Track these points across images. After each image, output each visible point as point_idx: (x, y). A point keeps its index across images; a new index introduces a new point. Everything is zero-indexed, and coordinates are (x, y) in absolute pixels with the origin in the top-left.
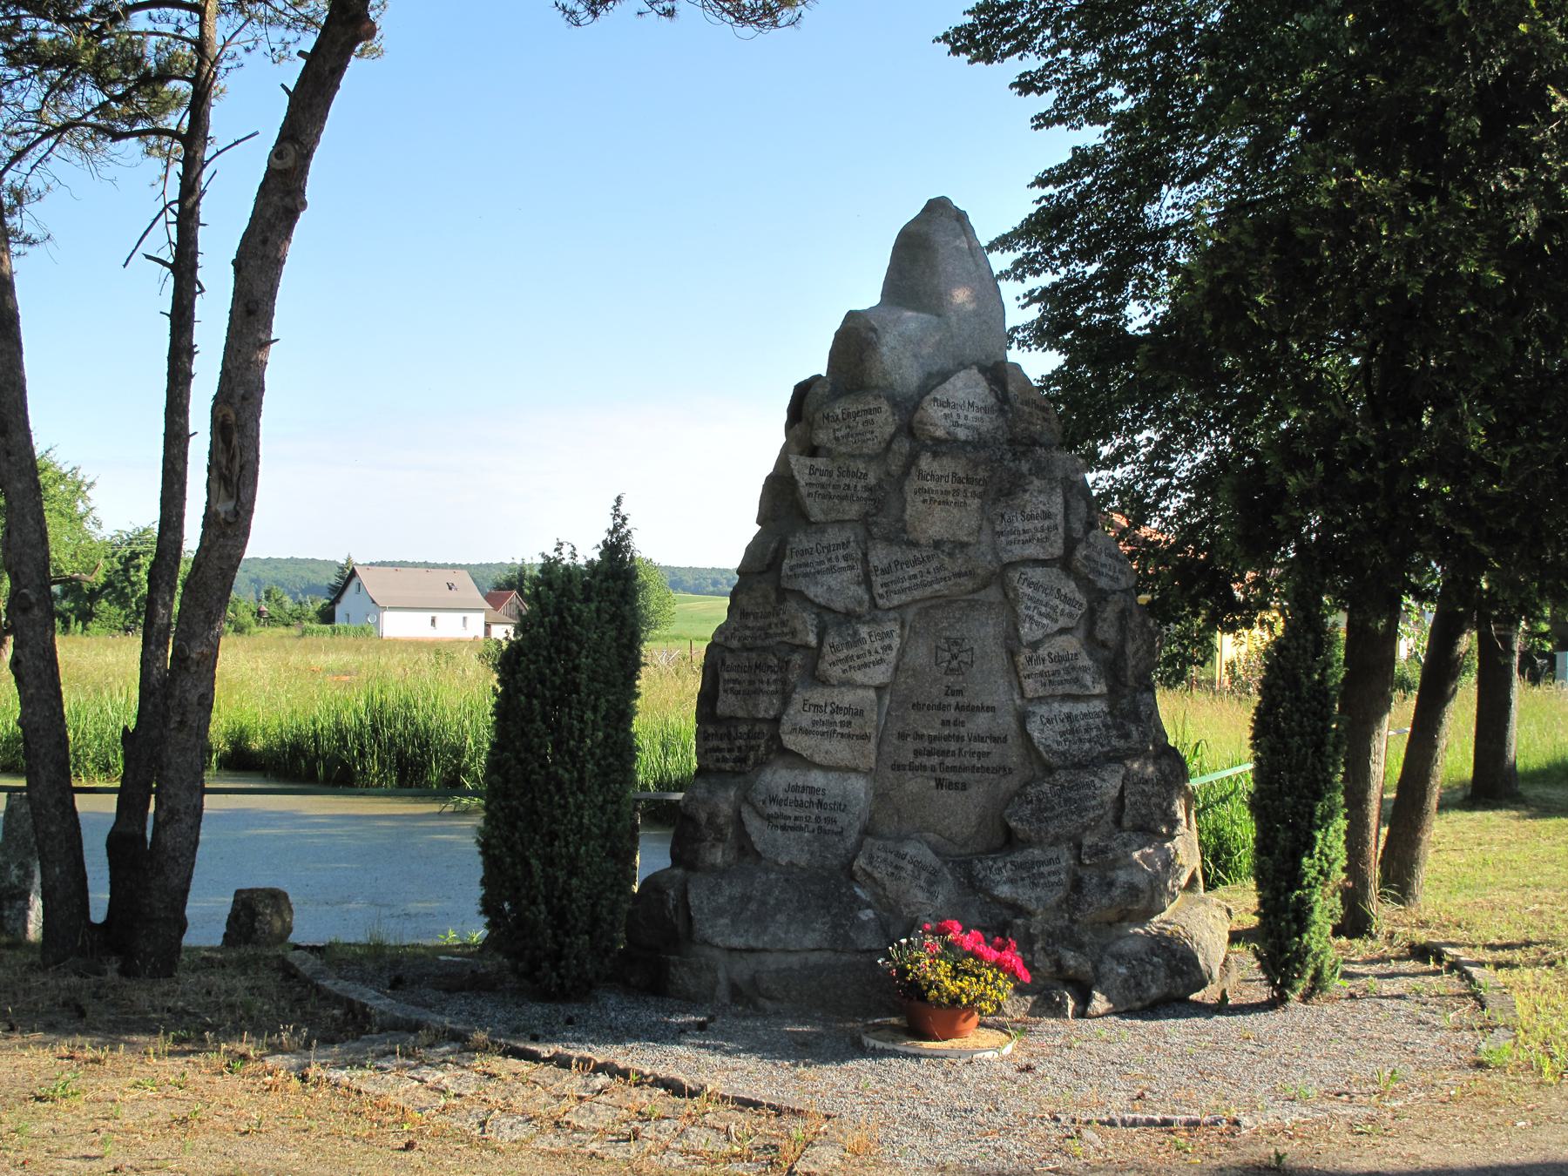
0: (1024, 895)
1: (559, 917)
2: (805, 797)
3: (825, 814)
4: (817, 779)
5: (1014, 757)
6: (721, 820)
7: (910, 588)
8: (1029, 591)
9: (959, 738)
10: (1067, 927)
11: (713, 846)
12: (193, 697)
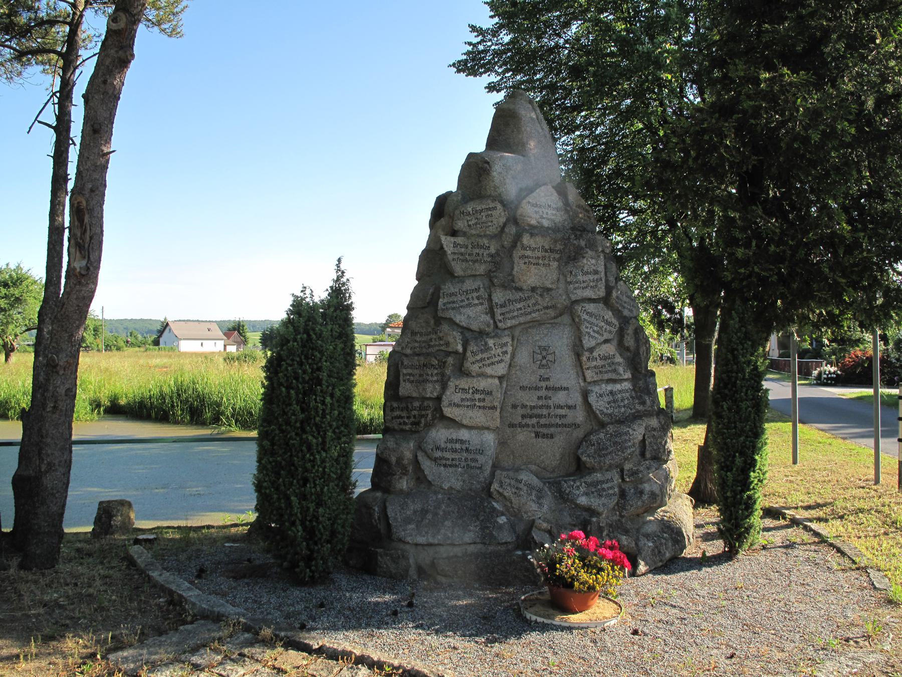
0: (595, 502)
1: (311, 533)
2: (458, 446)
3: (470, 456)
4: (464, 434)
5: (579, 416)
6: (405, 462)
7: (517, 316)
8: (586, 317)
10: (619, 520)
11: (401, 478)
12: (62, 390)
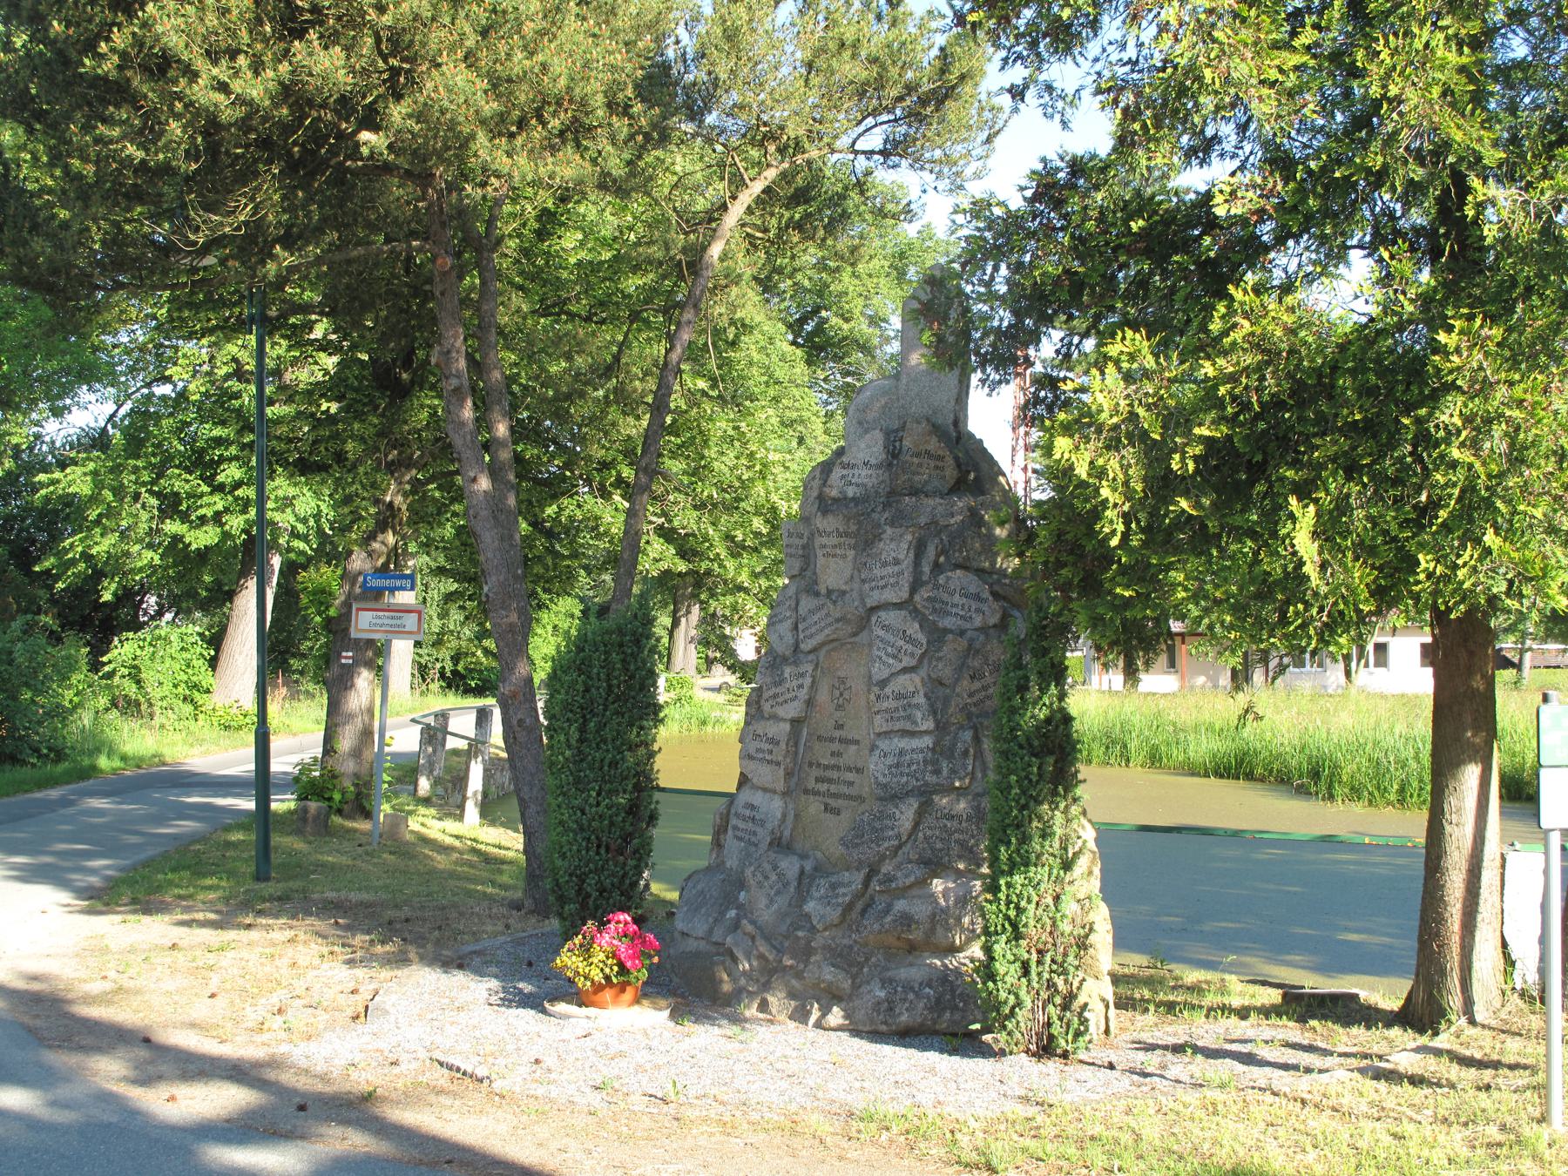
9: (839, 768)
